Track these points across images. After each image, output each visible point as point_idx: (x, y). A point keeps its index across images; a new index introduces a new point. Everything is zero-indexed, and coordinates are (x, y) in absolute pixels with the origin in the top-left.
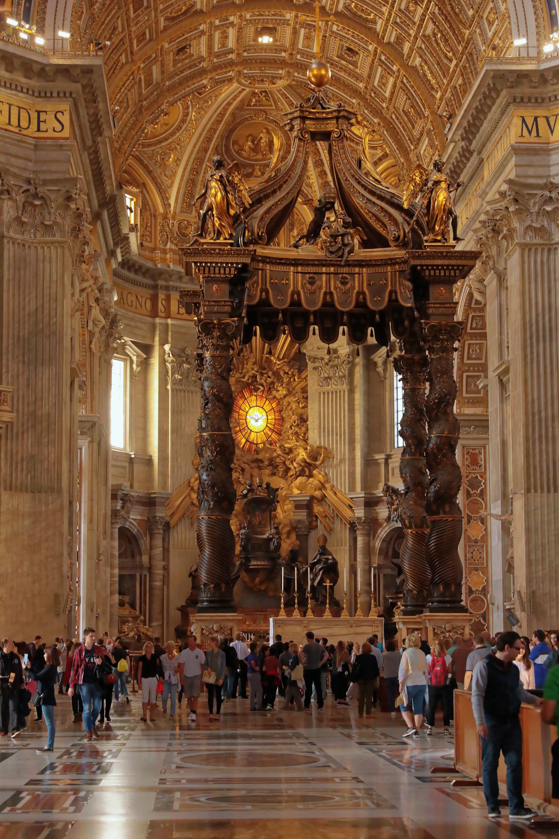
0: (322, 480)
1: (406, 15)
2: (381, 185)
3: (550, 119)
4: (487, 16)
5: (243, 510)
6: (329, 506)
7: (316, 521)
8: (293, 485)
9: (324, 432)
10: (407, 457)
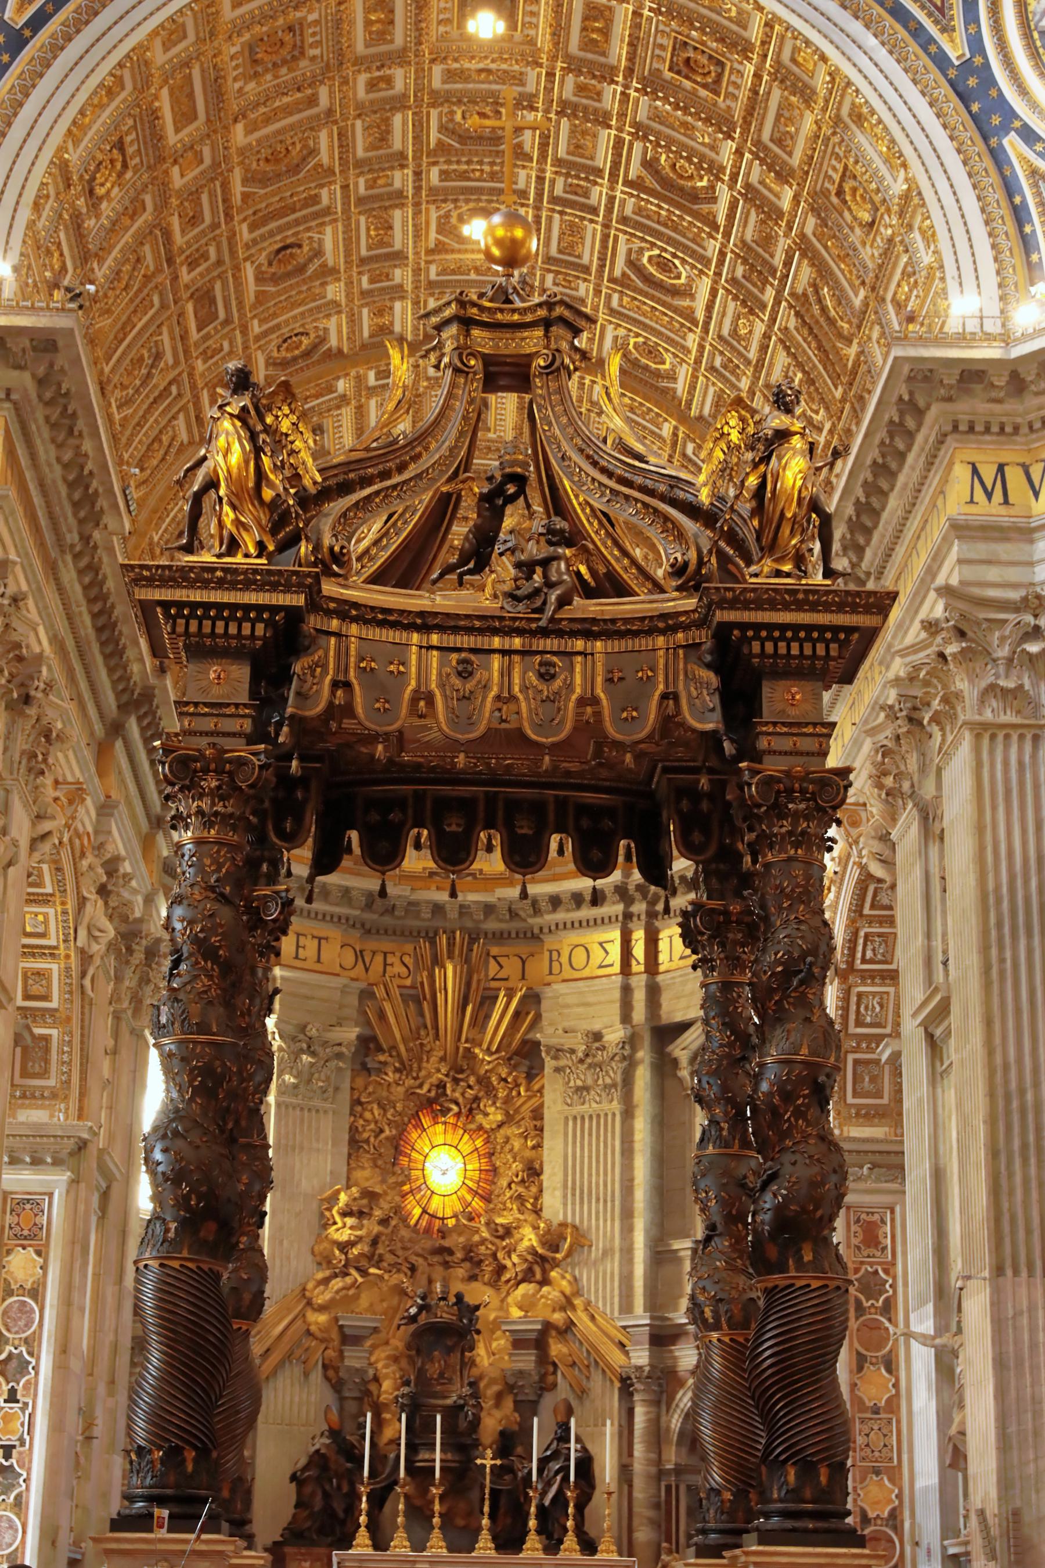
0: (568, 1291)
1: (732, 347)
2: (647, 462)
3: (1031, 470)
4: (895, 293)
5: (409, 1347)
6: (581, 1343)
7: (555, 1373)
8: (510, 1299)
9: (573, 1195)
10: (710, 1149)
